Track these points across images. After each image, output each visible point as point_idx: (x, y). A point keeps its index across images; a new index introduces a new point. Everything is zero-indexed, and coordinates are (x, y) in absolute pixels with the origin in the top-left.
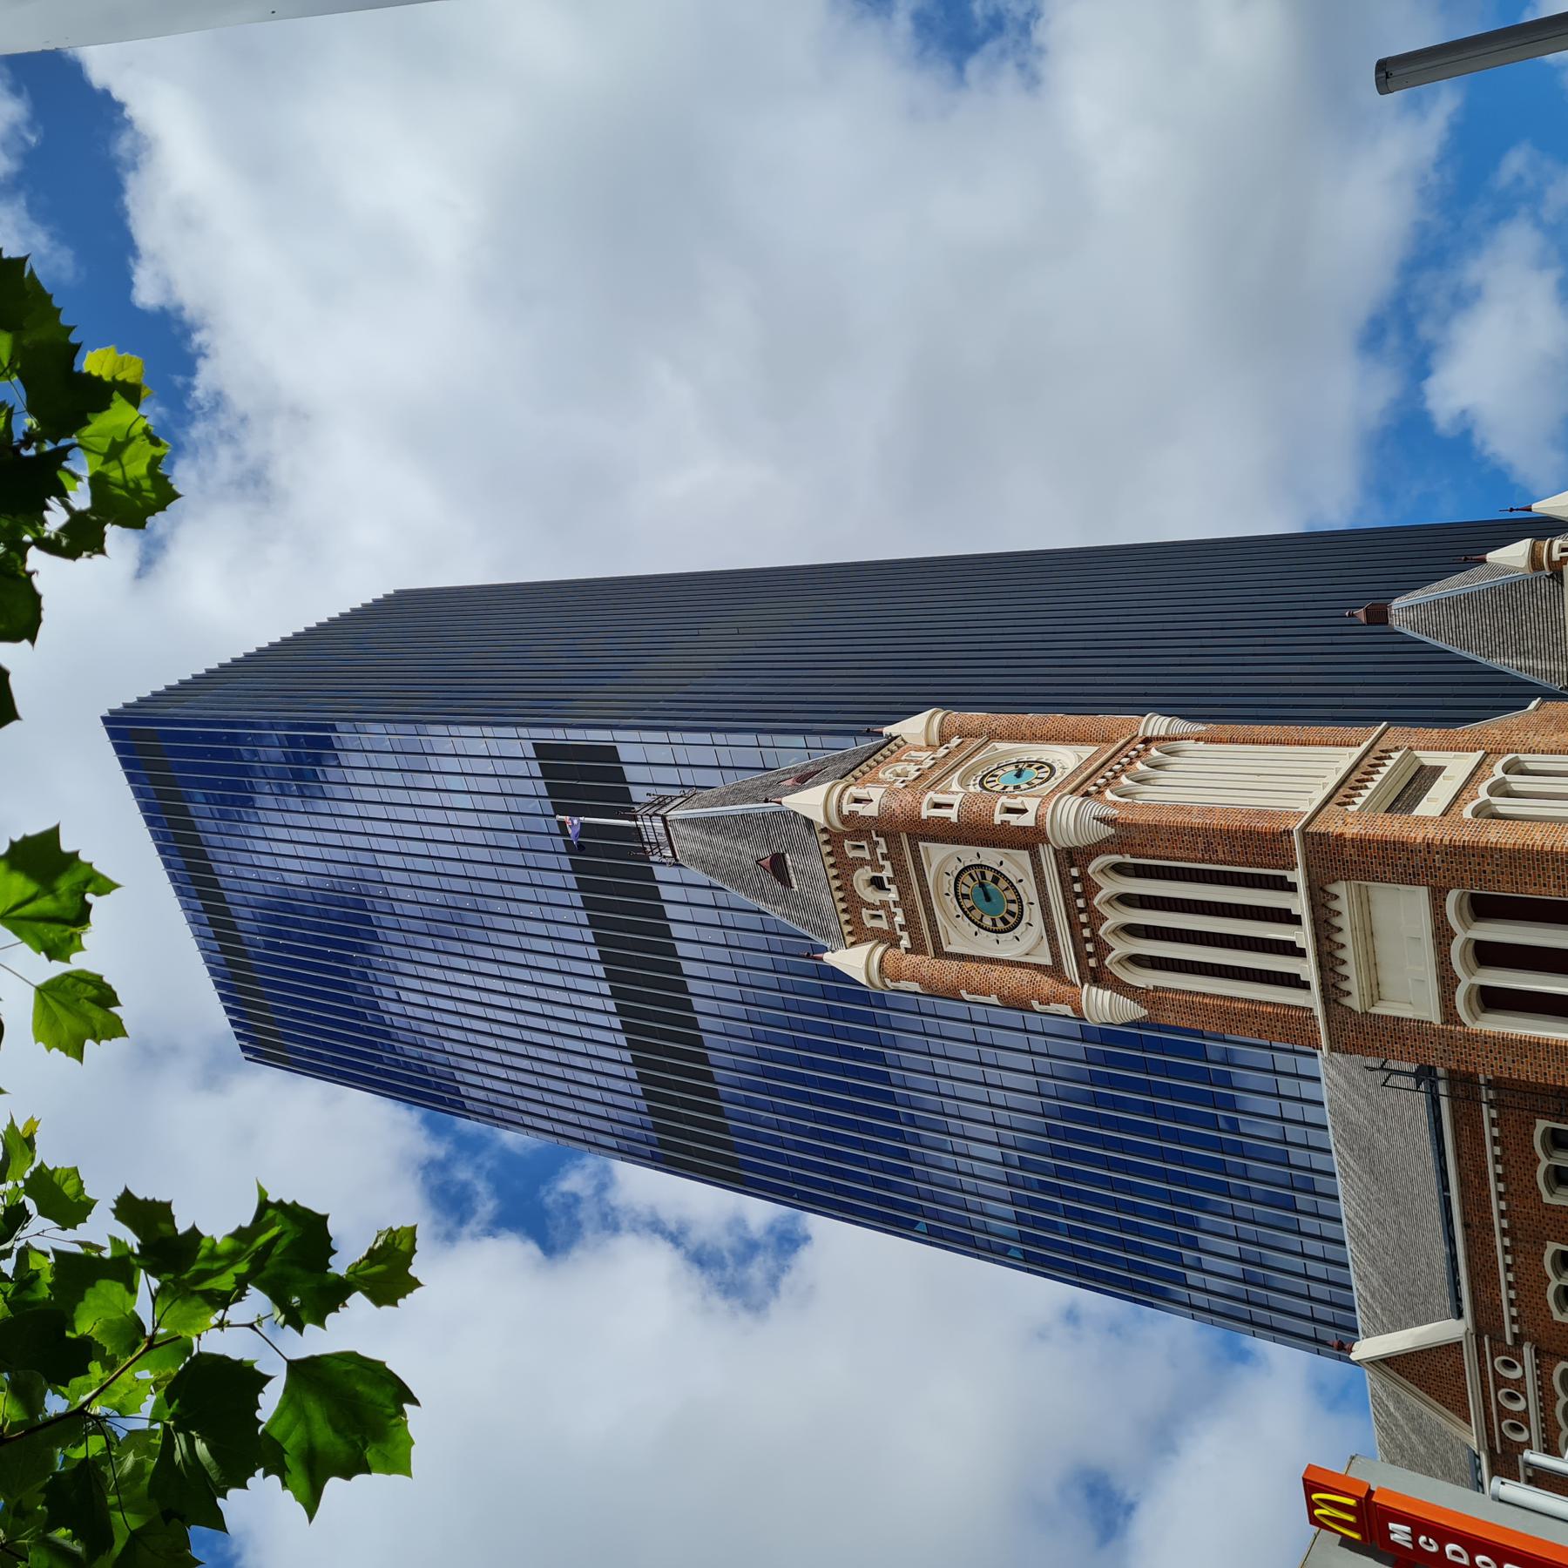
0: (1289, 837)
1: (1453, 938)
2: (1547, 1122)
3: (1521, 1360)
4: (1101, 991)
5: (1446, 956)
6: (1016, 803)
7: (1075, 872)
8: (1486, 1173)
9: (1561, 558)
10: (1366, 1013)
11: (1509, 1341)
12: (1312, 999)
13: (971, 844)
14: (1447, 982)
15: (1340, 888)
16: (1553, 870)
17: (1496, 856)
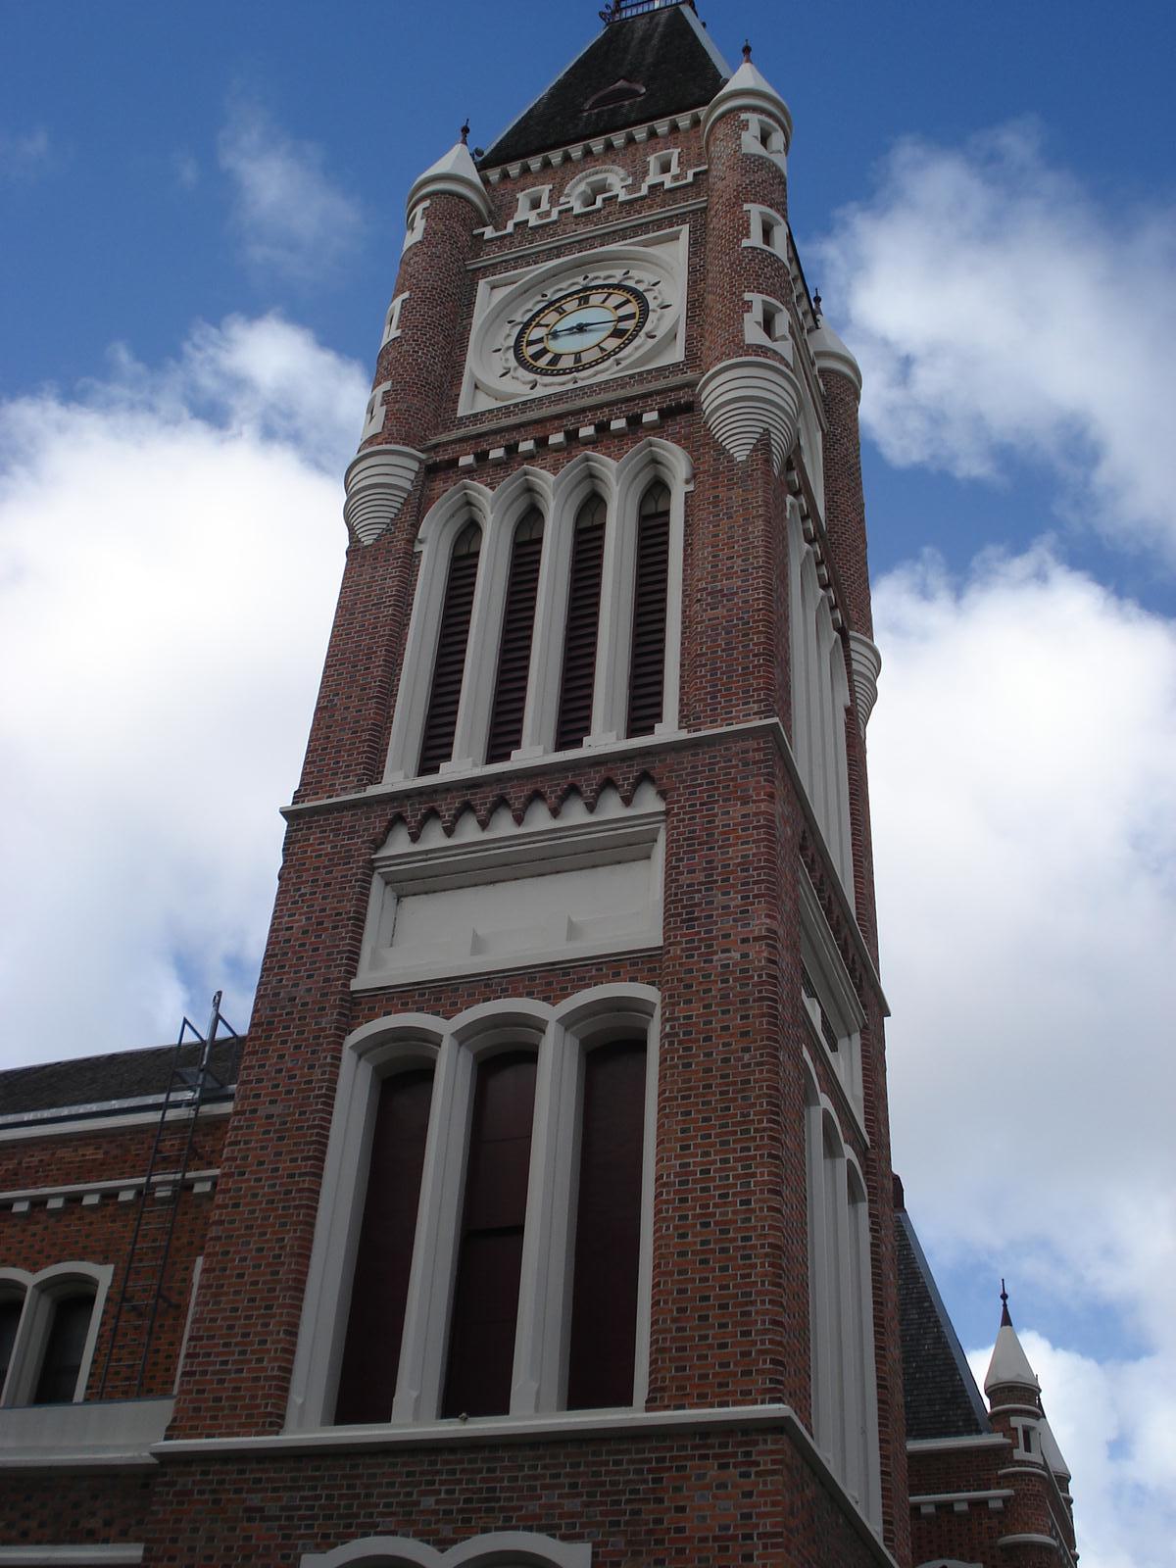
0: (755, 714)
1: (546, 999)
2: (109, 1283)
5: (503, 990)
7: (650, 417)
8: (14, 1187)
9: (1016, 1429)
10: (373, 869)
12: (399, 776)
13: (692, 285)
14: (440, 994)
15: (649, 802)
16: (725, 1161)
17: (747, 1056)
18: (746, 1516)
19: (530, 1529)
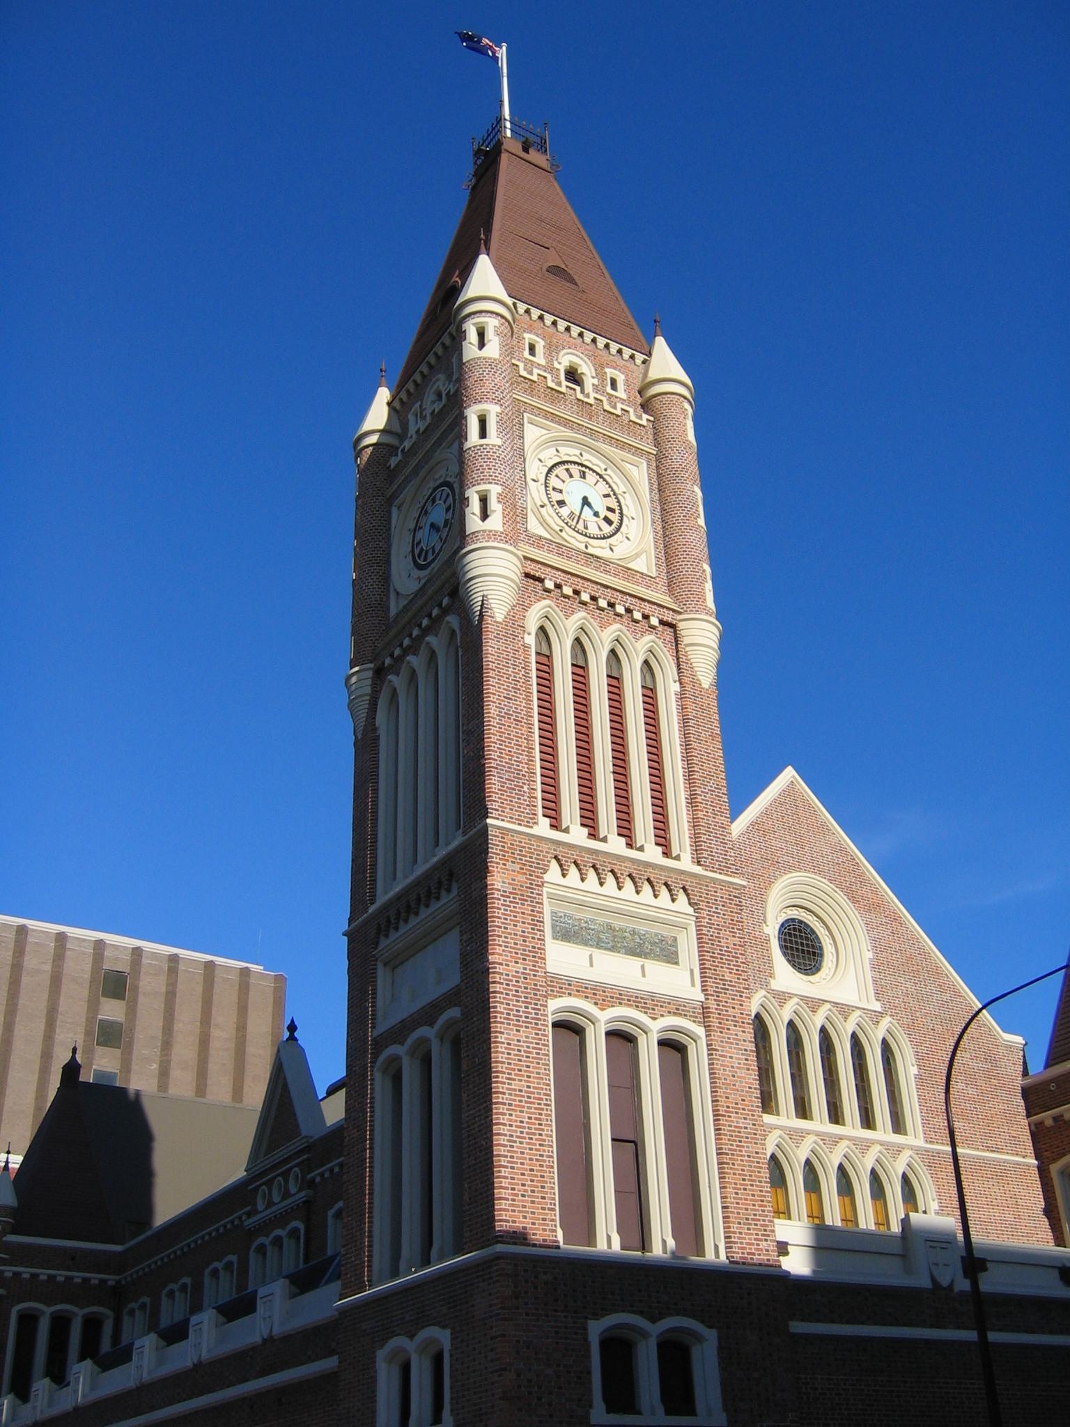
3: (300, 1190)
4: (369, 682)
6: (494, 505)
7: (446, 601)
10: (376, 960)
11: (309, 1176)
18: (490, 1306)
19: (434, 1325)
